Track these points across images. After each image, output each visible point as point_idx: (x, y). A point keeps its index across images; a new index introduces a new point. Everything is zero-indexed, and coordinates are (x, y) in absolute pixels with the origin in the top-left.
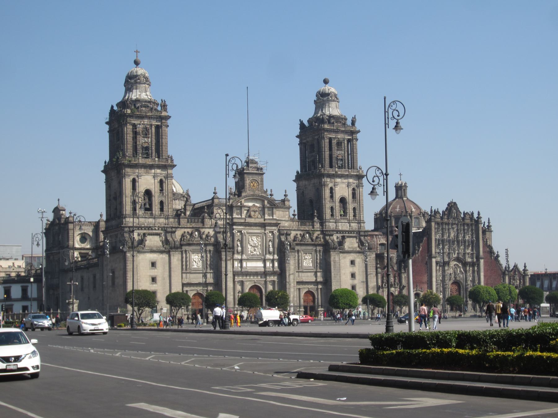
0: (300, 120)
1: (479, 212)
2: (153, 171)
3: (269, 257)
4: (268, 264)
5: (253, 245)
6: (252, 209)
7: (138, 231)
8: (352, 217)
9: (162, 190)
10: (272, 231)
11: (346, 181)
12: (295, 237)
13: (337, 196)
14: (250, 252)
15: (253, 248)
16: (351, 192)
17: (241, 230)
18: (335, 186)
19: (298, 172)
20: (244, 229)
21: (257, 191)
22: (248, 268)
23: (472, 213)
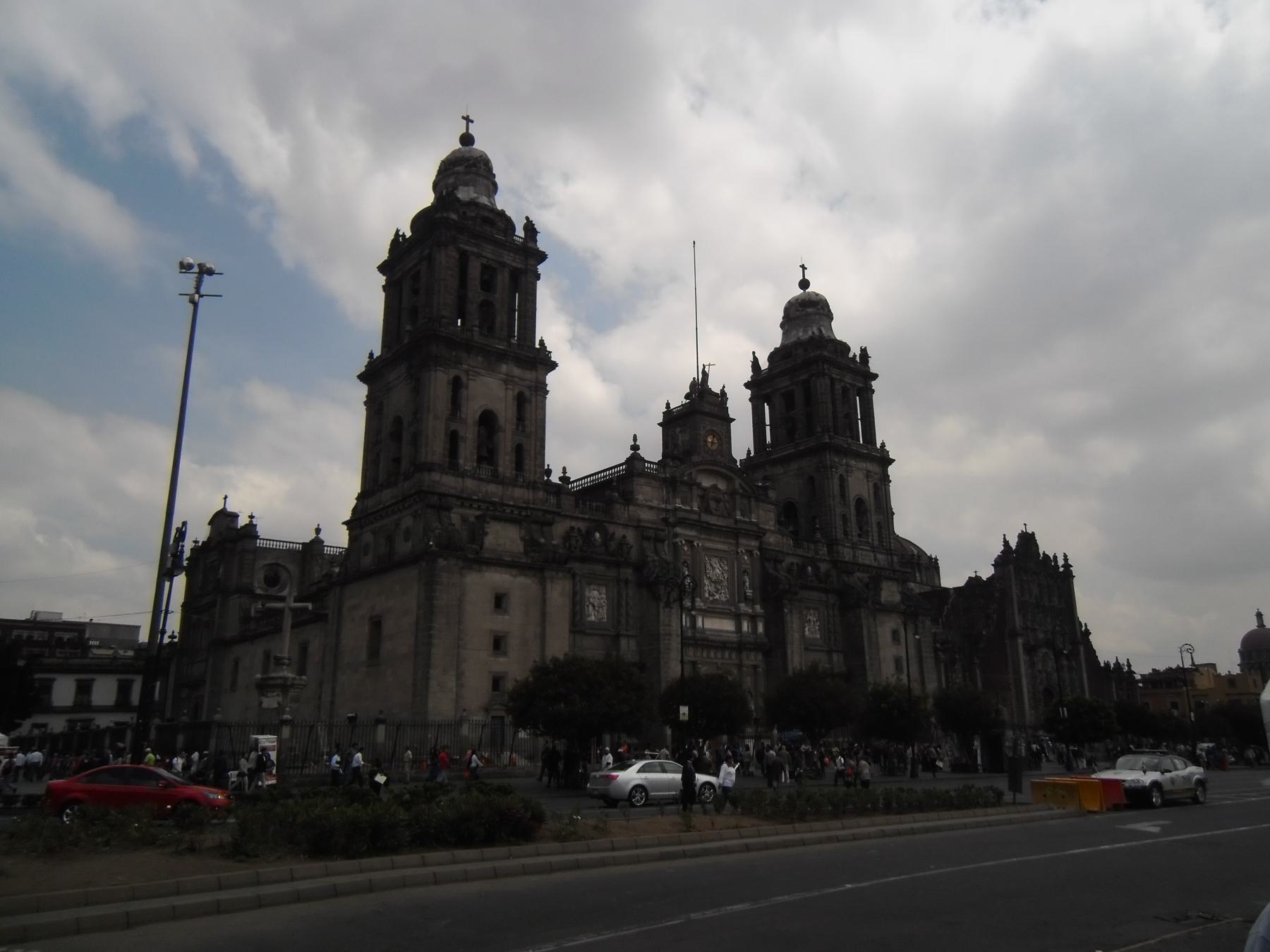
0: (754, 353)
1: (1065, 556)
2: (504, 368)
3: (742, 606)
4: (745, 626)
5: (714, 578)
6: (711, 494)
7: (460, 510)
8: (876, 543)
9: (520, 418)
10: (750, 549)
11: (863, 465)
12: (789, 571)
13: (853, 493)
14: (707, 595)
15: (712, 584)
16: (872, 492)
17: (691, 539)
18: (847, 472)
19: (749, 452)
20: (699, 539)
21: (719, 457)
22: (707, 632)
23: (1055, 557)
